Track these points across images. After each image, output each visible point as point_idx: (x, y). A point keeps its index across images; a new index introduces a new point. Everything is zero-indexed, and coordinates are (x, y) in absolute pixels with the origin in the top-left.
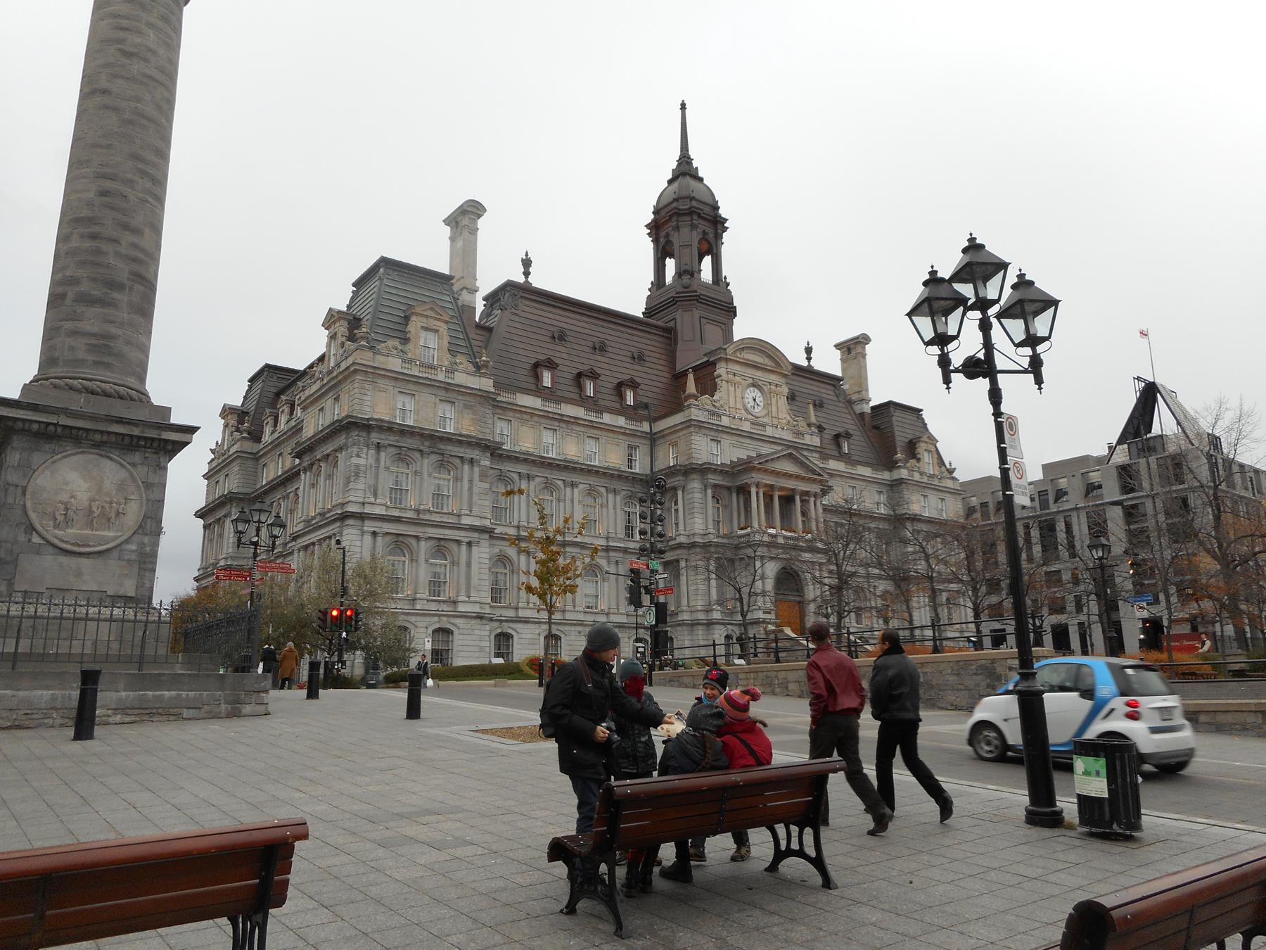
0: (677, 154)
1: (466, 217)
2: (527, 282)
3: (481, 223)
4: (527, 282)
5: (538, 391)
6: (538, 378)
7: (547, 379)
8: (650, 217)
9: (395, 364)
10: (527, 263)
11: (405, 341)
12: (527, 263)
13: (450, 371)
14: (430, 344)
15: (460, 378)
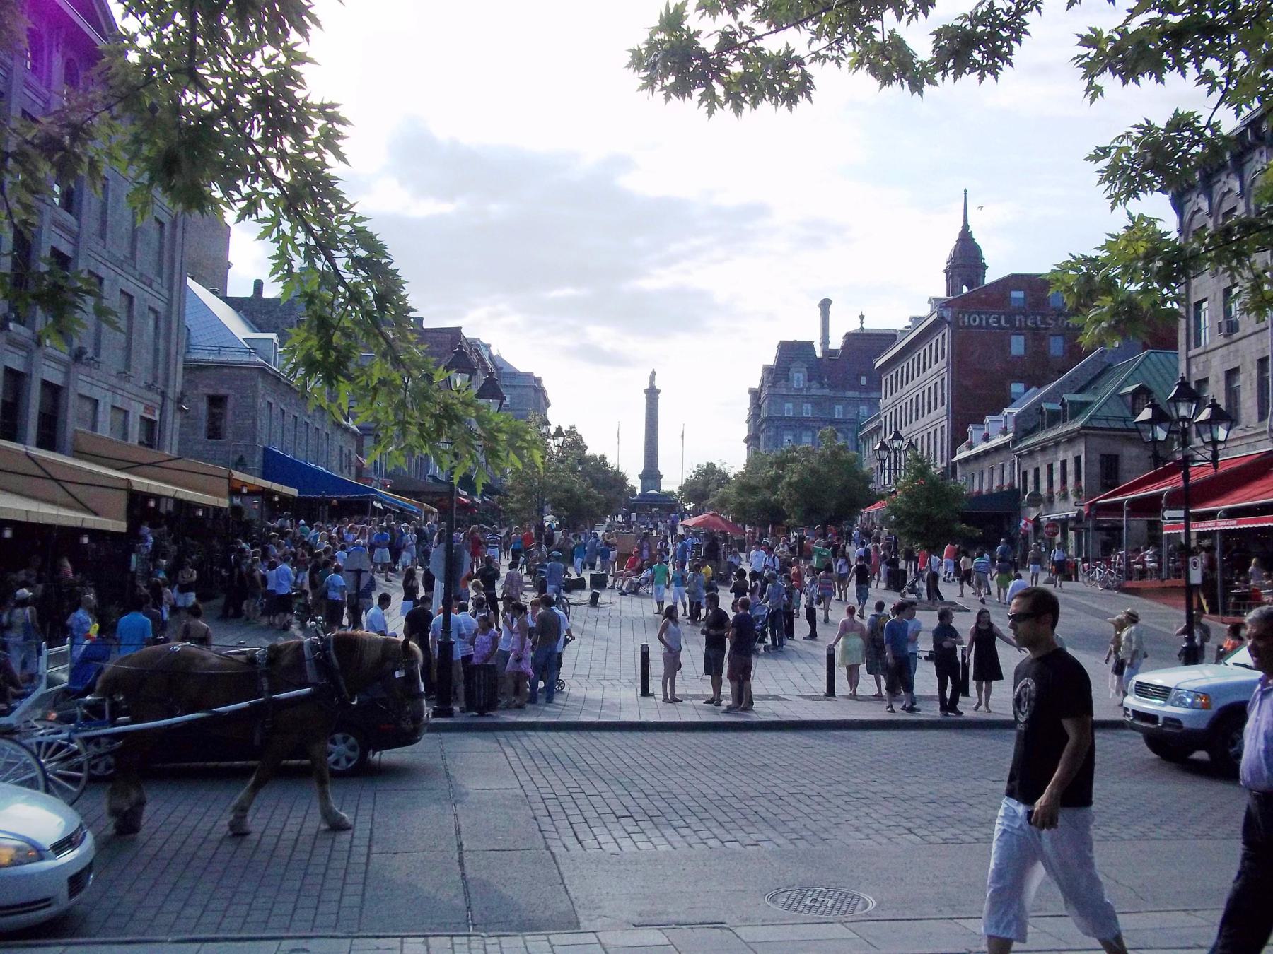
0: (962, 223)
1: (825, 305)
2: (862, 328)
3: (831, 309)
4: (862, 328)
5: (858, 387)
6: (858, 380)
7: (863, 381)
8: (944, 266)
9: (784, 391)
10: (862, 317)
11: (788, 380)
12: (862, 317)
13: (809, 389)
14: (798, 378)
15: (813, 392)
